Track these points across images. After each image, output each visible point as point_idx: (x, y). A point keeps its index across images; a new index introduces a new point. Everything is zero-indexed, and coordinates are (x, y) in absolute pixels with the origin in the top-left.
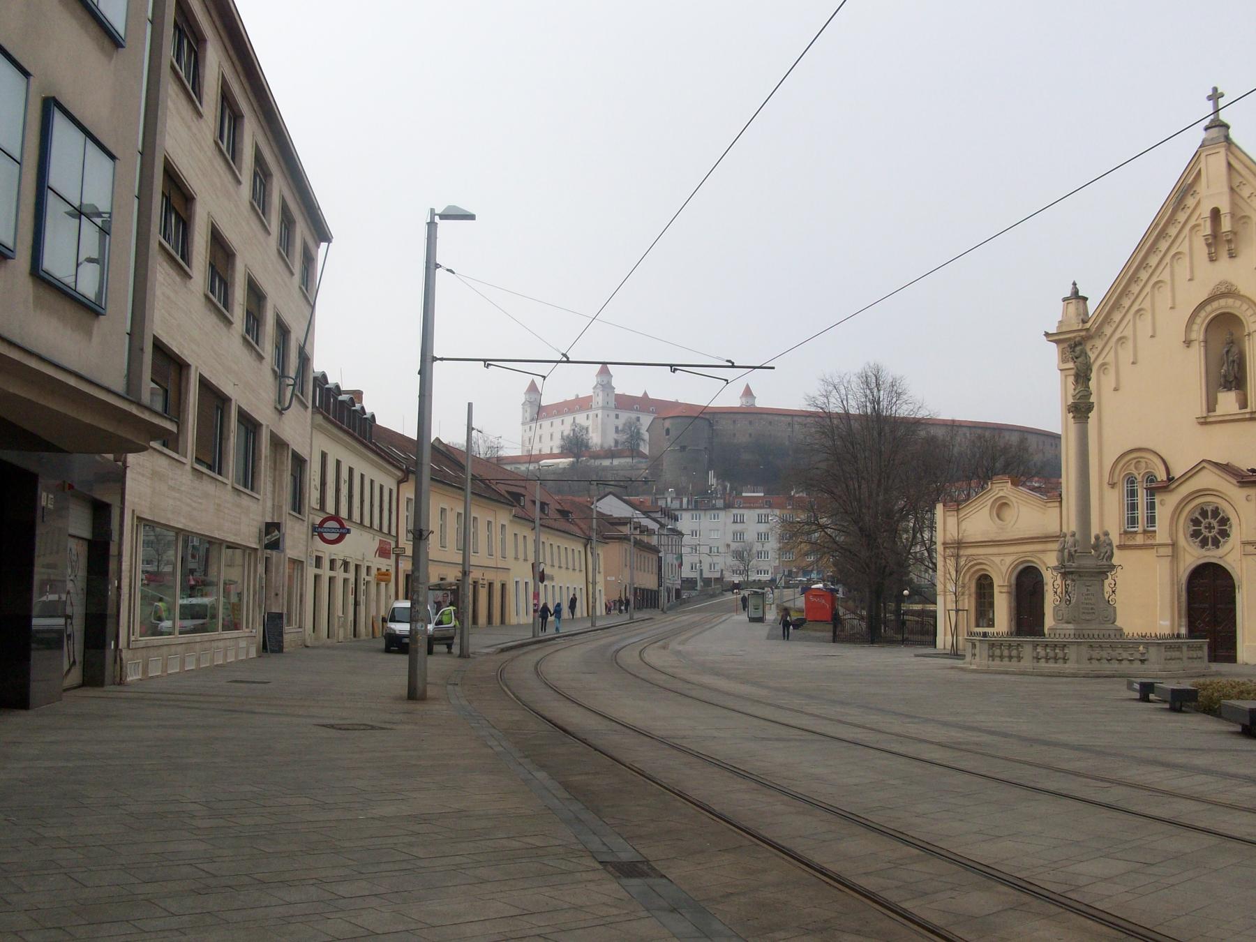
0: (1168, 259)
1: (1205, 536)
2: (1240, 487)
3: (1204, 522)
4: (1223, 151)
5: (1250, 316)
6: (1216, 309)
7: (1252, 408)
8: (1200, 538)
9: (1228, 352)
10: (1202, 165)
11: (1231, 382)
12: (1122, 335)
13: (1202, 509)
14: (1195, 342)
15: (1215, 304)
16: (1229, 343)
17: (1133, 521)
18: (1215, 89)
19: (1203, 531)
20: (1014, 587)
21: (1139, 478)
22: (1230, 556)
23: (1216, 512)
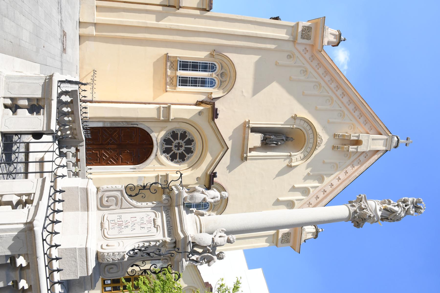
0: (343, 109)
1: (173, 142)
3: (182, 142)
9: (283, 140)
19: (177, 141)
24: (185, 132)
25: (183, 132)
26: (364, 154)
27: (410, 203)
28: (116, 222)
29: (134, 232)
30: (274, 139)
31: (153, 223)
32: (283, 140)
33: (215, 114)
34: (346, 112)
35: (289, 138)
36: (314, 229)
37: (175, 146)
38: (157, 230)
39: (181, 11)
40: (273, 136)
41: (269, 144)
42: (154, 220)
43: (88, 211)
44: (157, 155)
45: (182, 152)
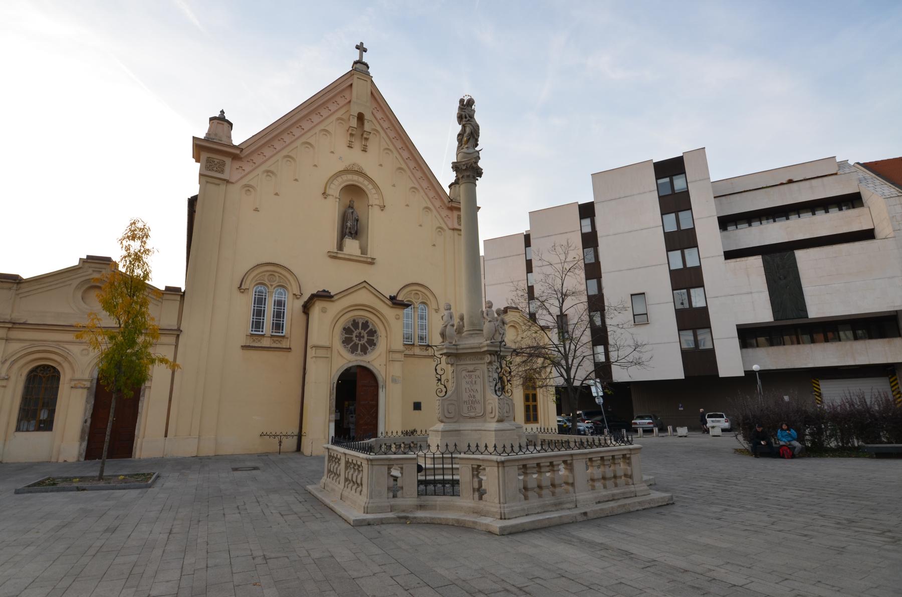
2: (392, 307)
4: (369, 81)
6: (350, 180)
8: (351, 345)
9: (352, 213)
10: (356, 82)
14: (331, 197)
15: (350, 177)
17: (258, 325)
18: (362, 44)
19: (354, 338)
22: (375, 360)
23: (365, 325)
24: (344, 329)
25: (344, 332)
26: (374, 112)
27: (463, 113)
28: (469, 406)
29: (479, 390)
31: (471, 373)
32: (352, 213)
33: (324, 296)
34: (322, 127)
35: (350, 205)
37: (360, 340)
38: (478, 369)
41: (357, 229)
42: (468, 372)
43: (460, 431)
44: (369, 362)
45: (366, 333)
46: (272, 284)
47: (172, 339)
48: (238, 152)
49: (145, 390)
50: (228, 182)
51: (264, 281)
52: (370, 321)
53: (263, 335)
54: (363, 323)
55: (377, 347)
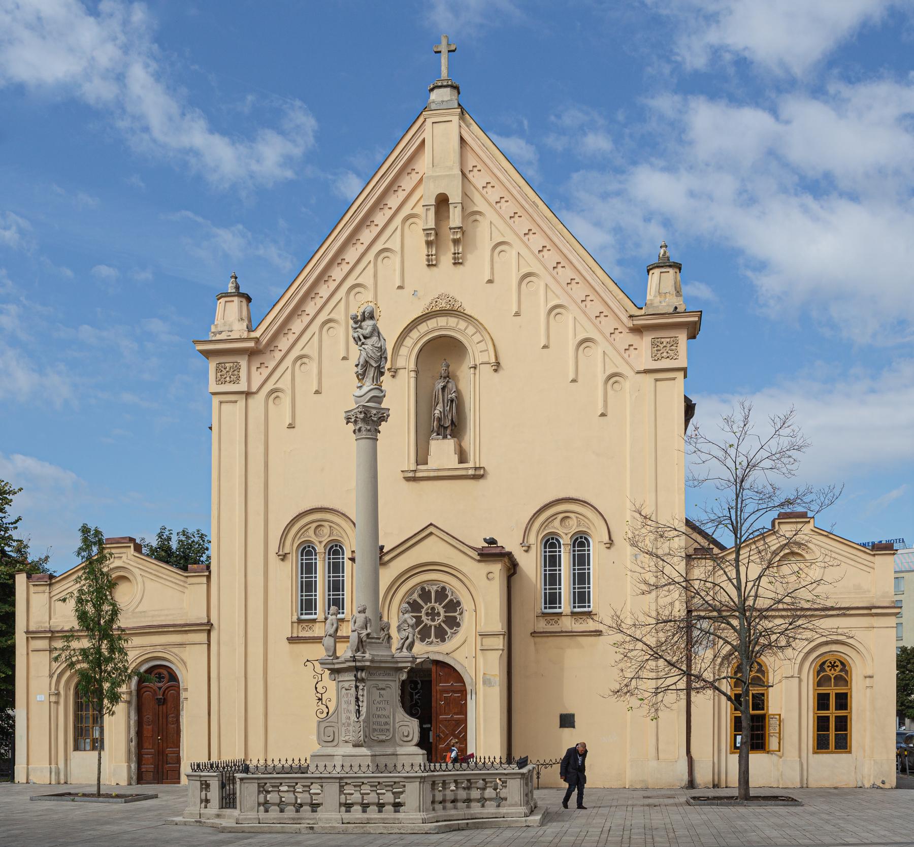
1: (426, 625)
3: (426, 607)
5: (478, 343)
7: (475, 463)
9: (444, 388)
11: (446, 428)
12: (303, 353)
13: (423, 589)
15: (432, 323)
16: (445, 378)
17: (308, 605)
20: (134, 693)
21: (320, 548)
23: (442, 594)
30: (441, 410)
36: (653, 273)
37: (433, 620)
39: (214, 620)
40: (437, 412)
45: (443, 607)
46: (321, 540)
47: (203, 637)
48: (251, 344)
49: (183, 703)
50: (248, 394)
51: (310, 537)
52: (448, 587)
53: (314, 621)
54: (437, 591)
55: (463, 630)
